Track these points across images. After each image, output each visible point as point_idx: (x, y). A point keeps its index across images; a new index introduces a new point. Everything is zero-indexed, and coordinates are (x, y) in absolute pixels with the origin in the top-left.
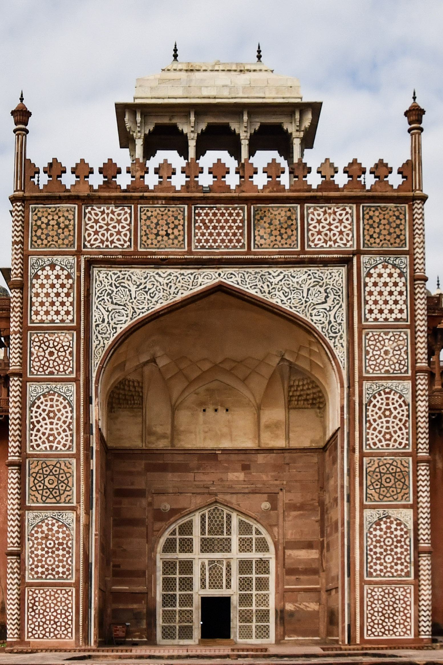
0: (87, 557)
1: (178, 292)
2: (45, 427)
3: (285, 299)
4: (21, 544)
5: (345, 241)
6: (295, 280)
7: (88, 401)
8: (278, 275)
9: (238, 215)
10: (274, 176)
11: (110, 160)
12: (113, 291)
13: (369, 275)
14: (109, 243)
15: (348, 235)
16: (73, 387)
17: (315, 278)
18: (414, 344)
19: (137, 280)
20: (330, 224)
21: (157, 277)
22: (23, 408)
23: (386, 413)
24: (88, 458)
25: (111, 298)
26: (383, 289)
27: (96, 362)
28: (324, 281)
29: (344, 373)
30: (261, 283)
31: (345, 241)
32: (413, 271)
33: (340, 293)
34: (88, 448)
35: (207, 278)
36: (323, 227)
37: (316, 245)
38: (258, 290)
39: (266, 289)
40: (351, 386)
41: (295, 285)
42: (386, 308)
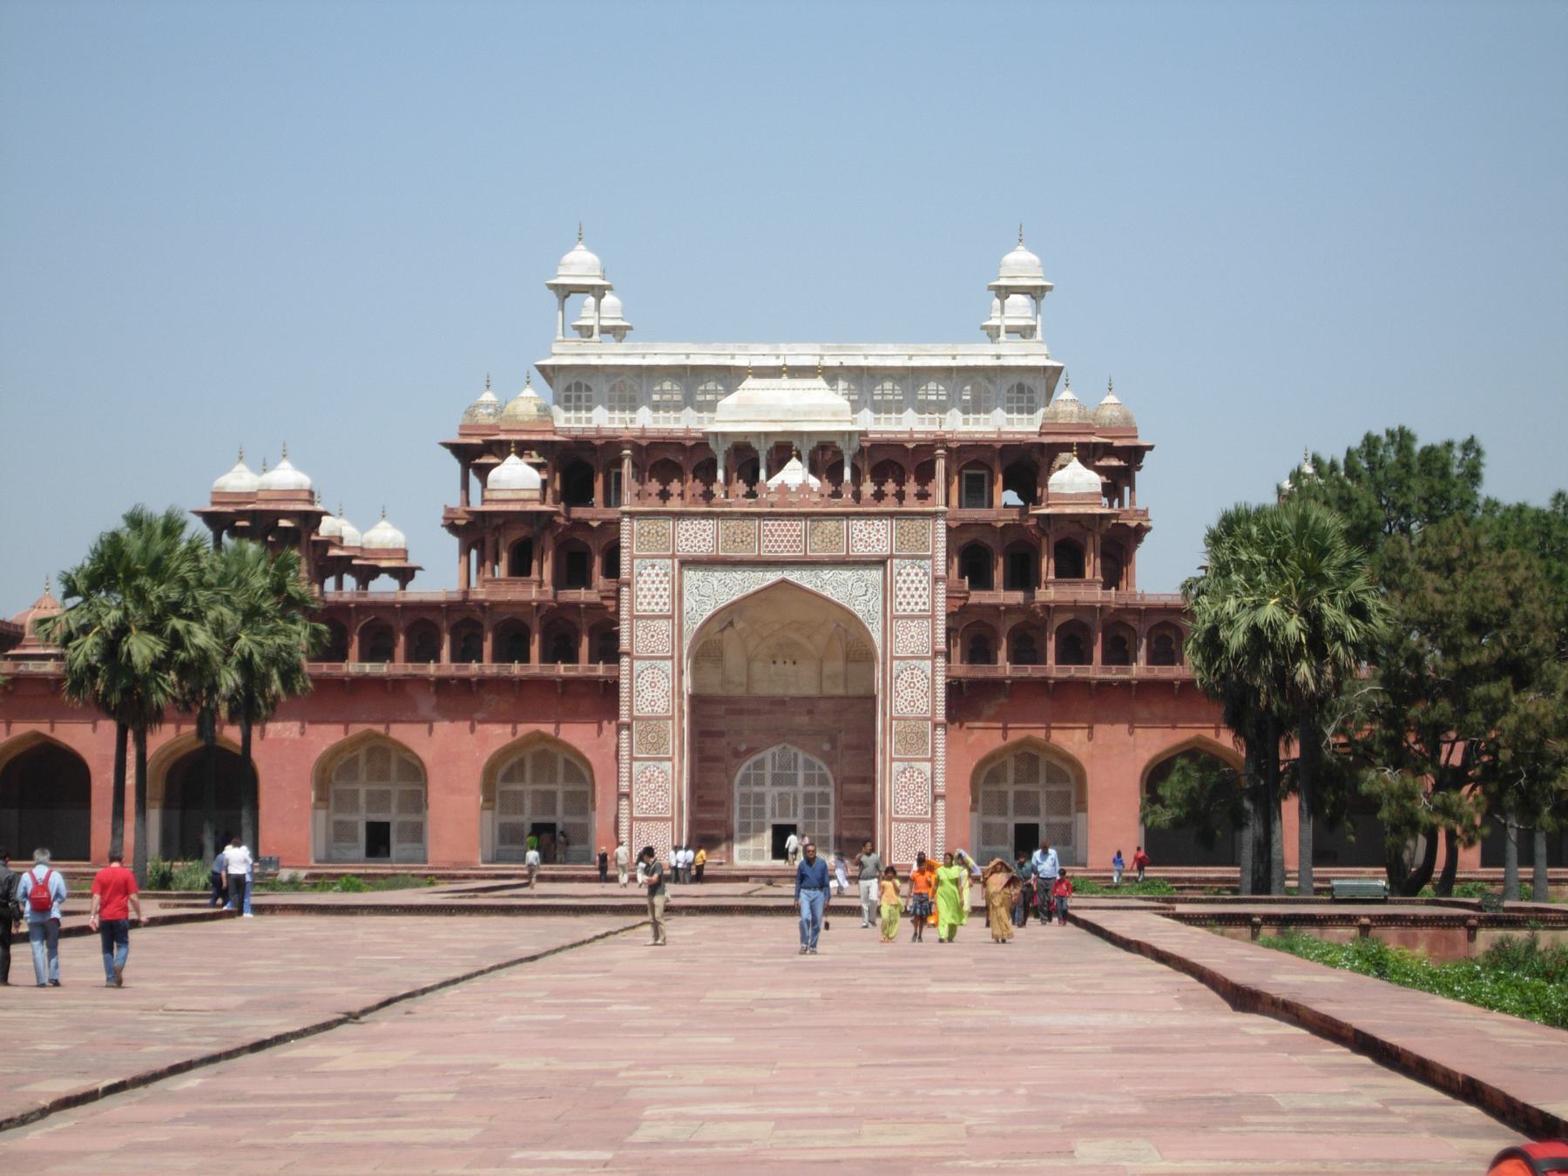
0: (680, 797)
2: (648, 694)
4: (631, 786)
7: (681, 672)
13: (900, 574)
16: (669, 663)
18: (934, 630)
22: (631, 680)
23: (911, 685)
24: (681, 718)
27: (687, 643)
29: (880, 652)
32: (934, 570)
34: (681, 710)
35: (772, 577)
40: (884, 663)
42: (913, 601)
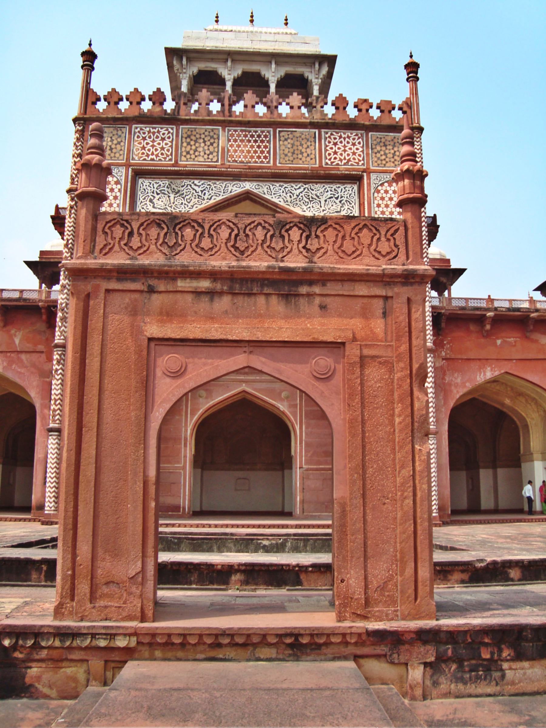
1: (211, 198)
3: (305, 208)
5: (357, 161)
6: (313, 192)
8: (300, 188)
9: (266, 136)
10: (296, 108)
11: (159, 89)
12: (154, 197)
14: (154, 157)
15: (360, 155)
17: (331, 191)
19: (176, 188)
20: (345, 146)
21: (193, 186)
25: (153, 203)
26: (389, 202)
28: (339, 194)
30: (284, 194)
31: (357, 161)
33: (353, 204)
36: (339, 148)
37: (332, 163)
38: (281, 199)
39: (289, 199)
41: (314, 197)
